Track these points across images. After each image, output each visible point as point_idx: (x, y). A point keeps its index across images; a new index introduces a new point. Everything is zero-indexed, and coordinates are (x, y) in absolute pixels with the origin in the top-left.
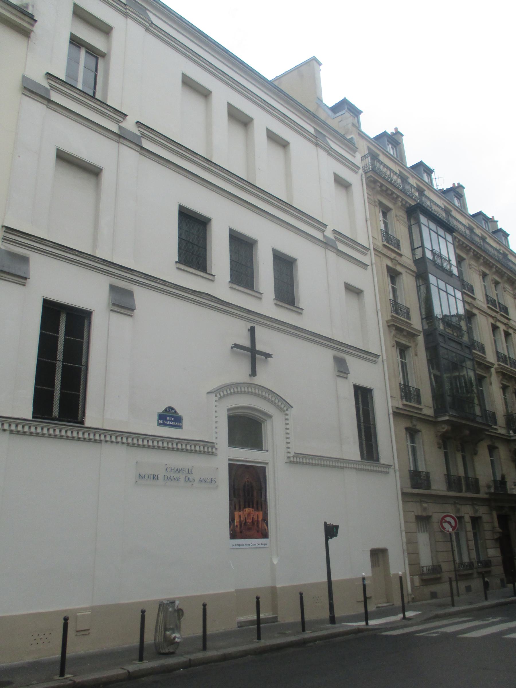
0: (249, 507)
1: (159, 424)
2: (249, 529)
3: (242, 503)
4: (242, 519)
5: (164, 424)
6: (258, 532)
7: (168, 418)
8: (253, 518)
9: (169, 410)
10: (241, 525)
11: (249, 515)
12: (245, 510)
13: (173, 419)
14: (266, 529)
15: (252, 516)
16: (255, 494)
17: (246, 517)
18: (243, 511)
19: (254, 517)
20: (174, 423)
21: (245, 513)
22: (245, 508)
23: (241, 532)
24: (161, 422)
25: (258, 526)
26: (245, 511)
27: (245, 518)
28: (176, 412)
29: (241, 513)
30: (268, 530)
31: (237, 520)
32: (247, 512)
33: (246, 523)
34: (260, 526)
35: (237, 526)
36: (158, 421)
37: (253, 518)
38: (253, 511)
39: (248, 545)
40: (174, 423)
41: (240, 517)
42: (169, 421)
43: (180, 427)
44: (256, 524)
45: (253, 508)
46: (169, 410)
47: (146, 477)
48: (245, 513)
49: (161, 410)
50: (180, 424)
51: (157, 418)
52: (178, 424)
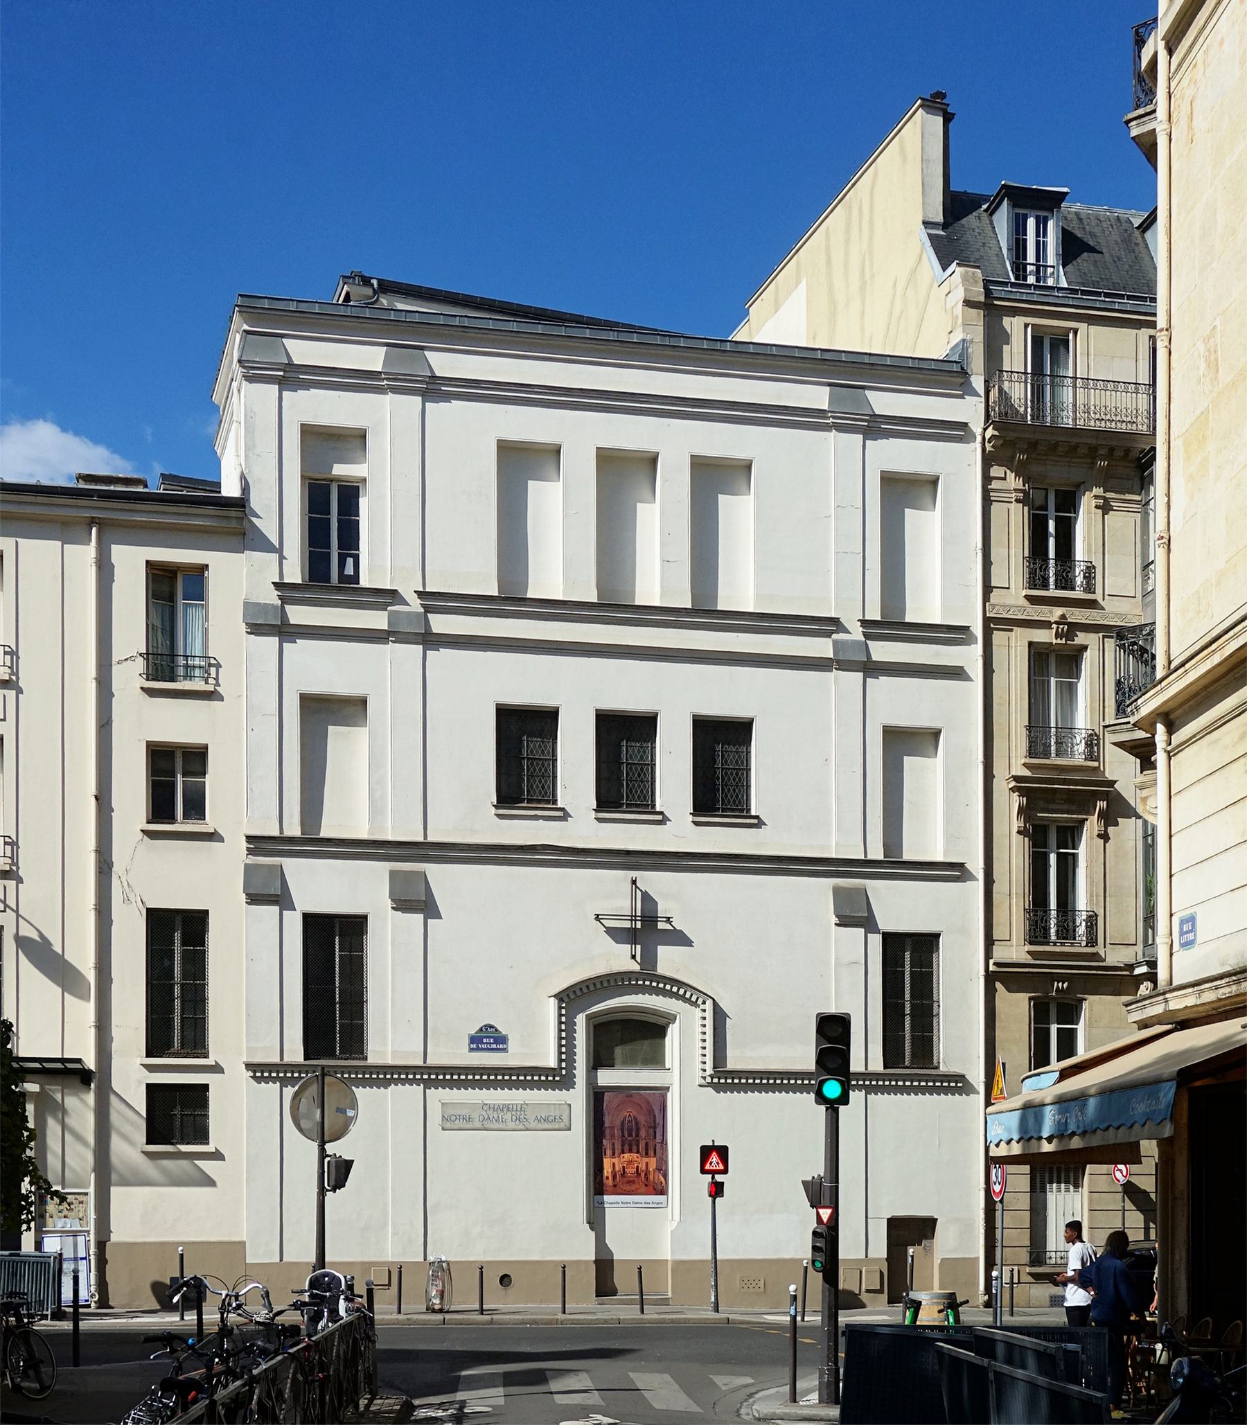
0: (630, 1151)
1: (472, 1050)
2: (631, 1182)
3: (618, 1147)
4: (617, 1169)
5: (478, 1049)
6: (646, 1185)
7: (485, 1041)
8: (638, 1167)
9: (487, 1029)
10: (614, 1177)
11: (630, 1162)
12: (622, 1156)
13: (492, 1041)
14: (662, 1183)
15: (636, 1165)
16: (643, 1133)
17: (625, 1165)
18: (619, 1157)
19: (640, 1166)
20: (494, 1046)
21: (622, 1160)
22: (623, 1152)
23: (615, 1186)
24: (474, 1046)
25: (647, 1179)
26: (623, 1157)
27: (624, 1167)
28: (496, 1030)
29: (616, 1160)
30: (667, 1183)
31: (607, 1171)
32: (625, 1159)
33: (623, 1174)
34: (651, 1177)
35: (607, 1178)
36: (469, 1045)
37: (638, 1167)
38: (638, 1157)
39: (627, 1203)
40: (494, 1046)
41: (614, 1165)
42: (487, 1043)
43: (505, 1050)
44: (643, 1175)
45: (638, 1152)
46: (487, 1029)
47: (453, 1118)
48: (622, 1160)
49: (473, 1032)
50: (505, 1046)
51: (467, 1041)
52: (501, 1046)
